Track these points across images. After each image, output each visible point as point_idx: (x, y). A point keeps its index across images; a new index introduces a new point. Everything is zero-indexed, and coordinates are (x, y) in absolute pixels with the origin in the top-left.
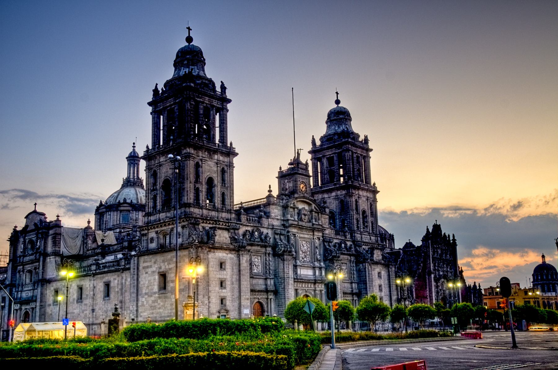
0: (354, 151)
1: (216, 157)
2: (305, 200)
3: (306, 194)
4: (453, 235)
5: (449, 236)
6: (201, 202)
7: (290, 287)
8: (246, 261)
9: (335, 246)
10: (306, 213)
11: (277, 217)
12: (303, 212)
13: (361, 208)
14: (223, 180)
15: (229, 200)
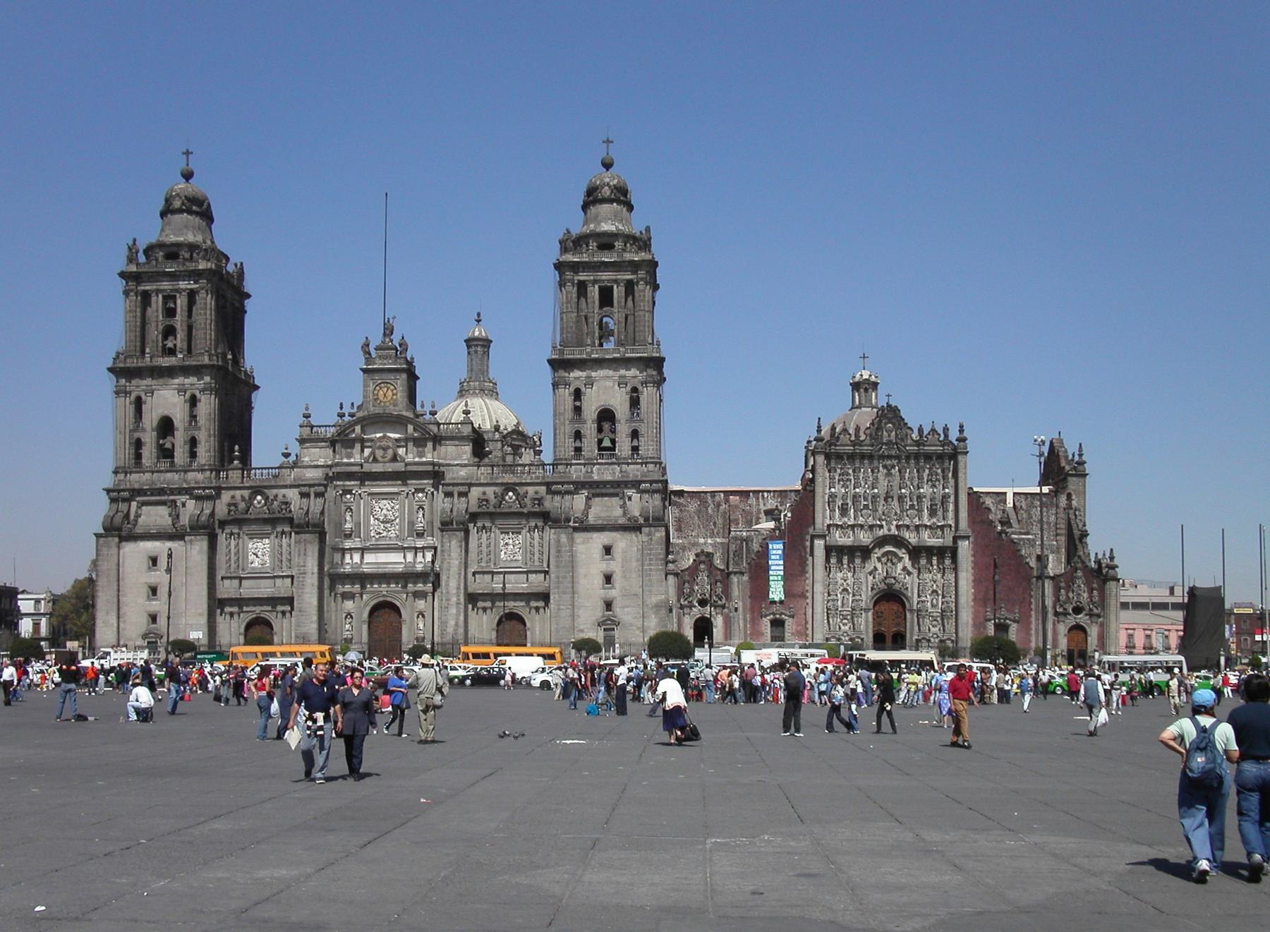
0: (582, 278)
1: (176, 381)
2: (385, 419)
3: (391, 407)
4: (961, 426)
5: (946, 429)
6: (144, 461)
7: (308, 589)
8: (200, 552)
9: (483, 501)
10: (390, 444)
11: (316, 463)
12: (378, 444)
13: (592, 406)
14: (193, 417)
15: (204, 449)
